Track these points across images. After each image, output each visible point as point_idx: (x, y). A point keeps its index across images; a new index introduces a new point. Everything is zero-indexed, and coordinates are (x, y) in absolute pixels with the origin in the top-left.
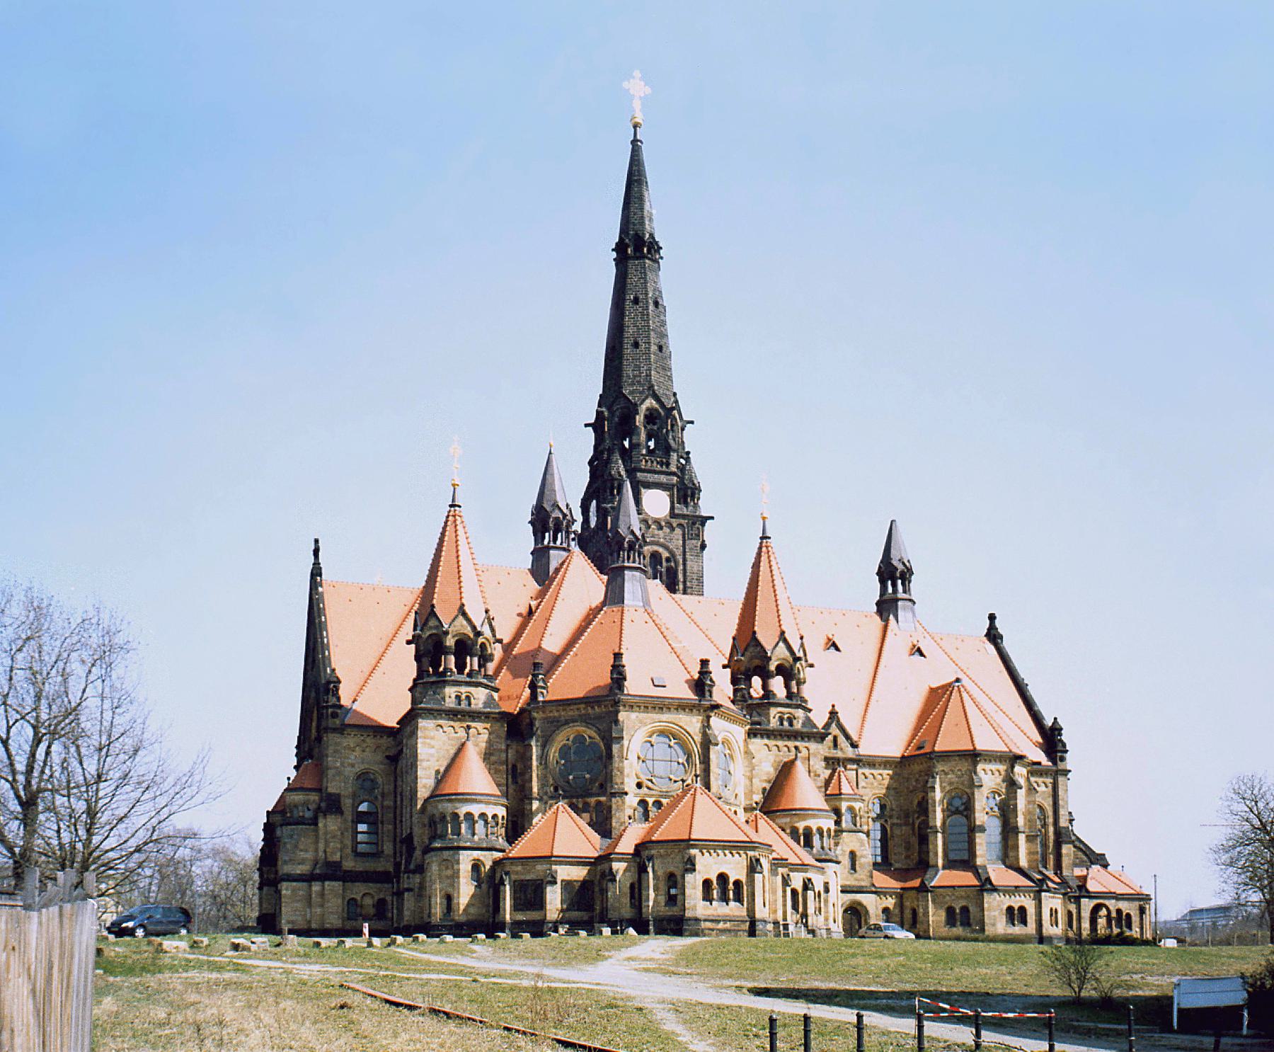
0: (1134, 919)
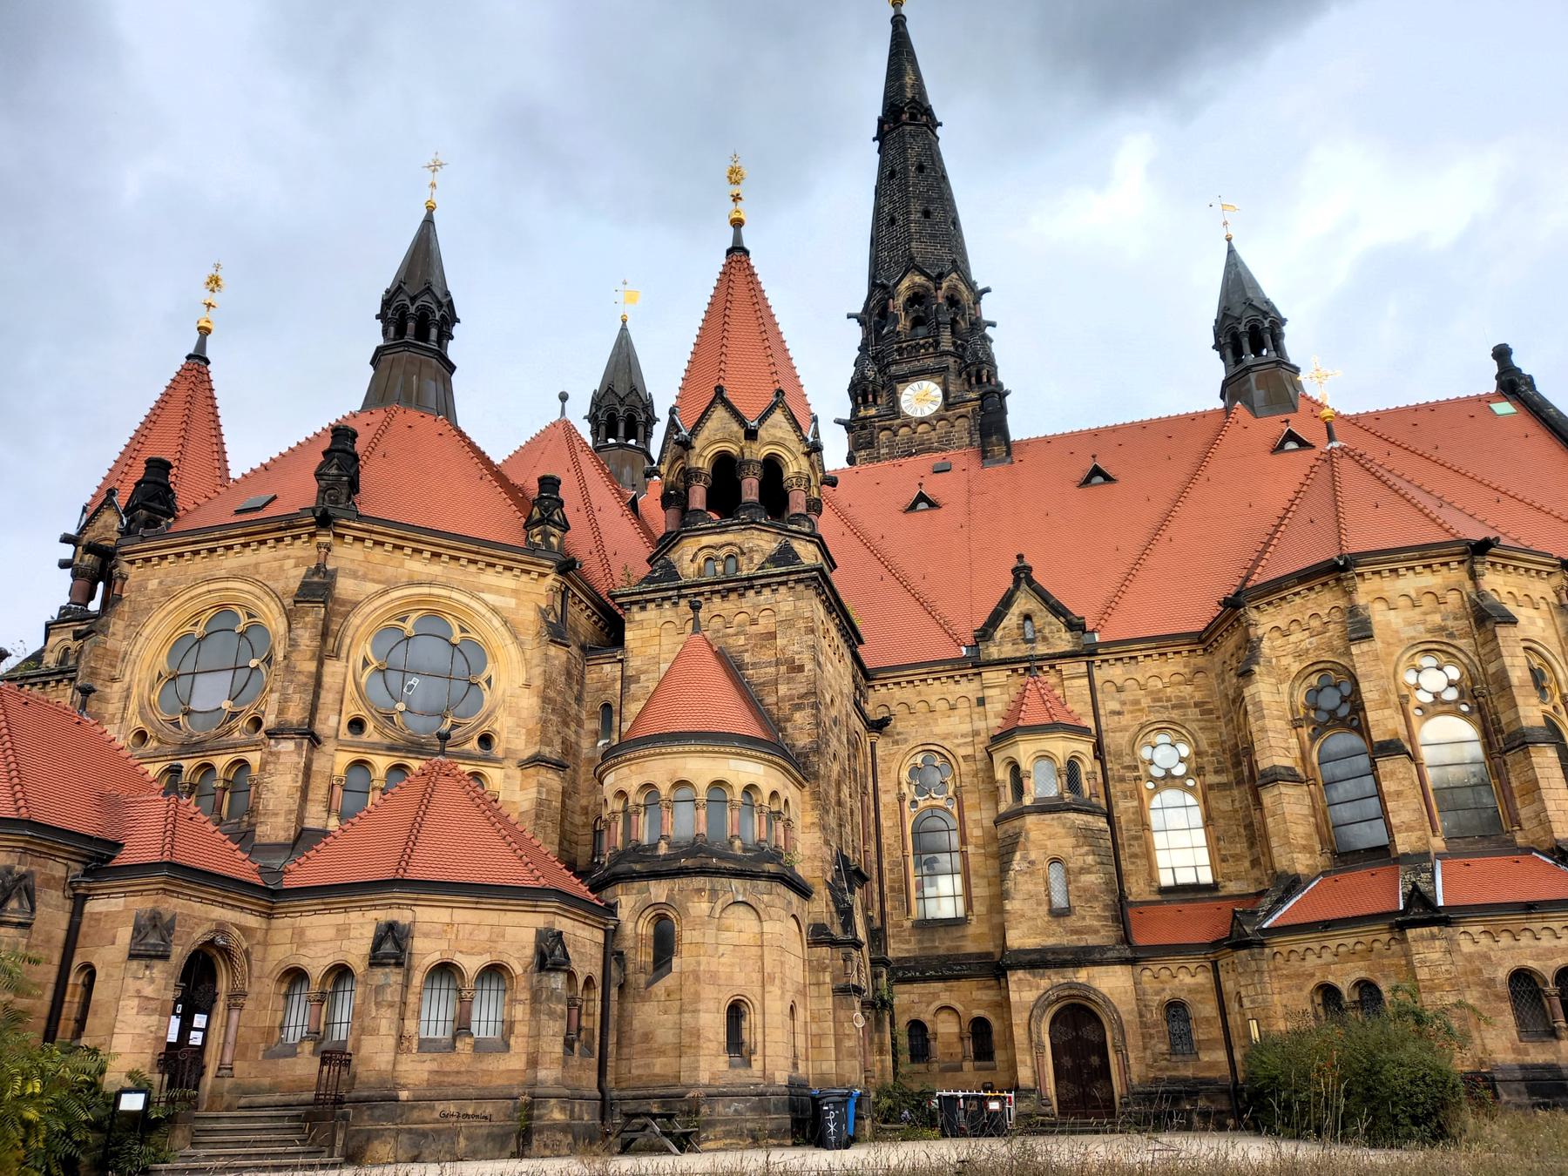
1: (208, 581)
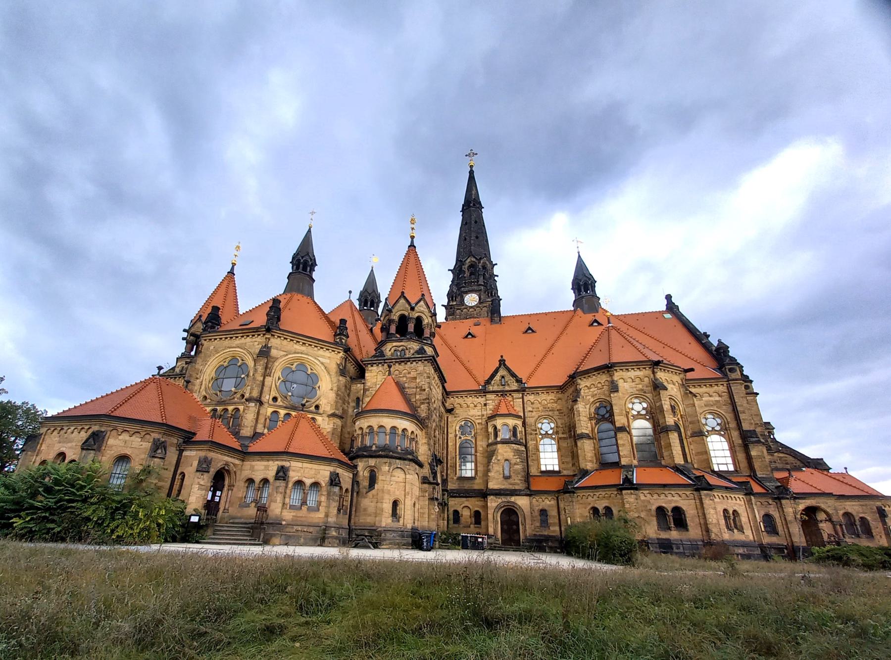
0: (873, 524)
1: (230, 348)
